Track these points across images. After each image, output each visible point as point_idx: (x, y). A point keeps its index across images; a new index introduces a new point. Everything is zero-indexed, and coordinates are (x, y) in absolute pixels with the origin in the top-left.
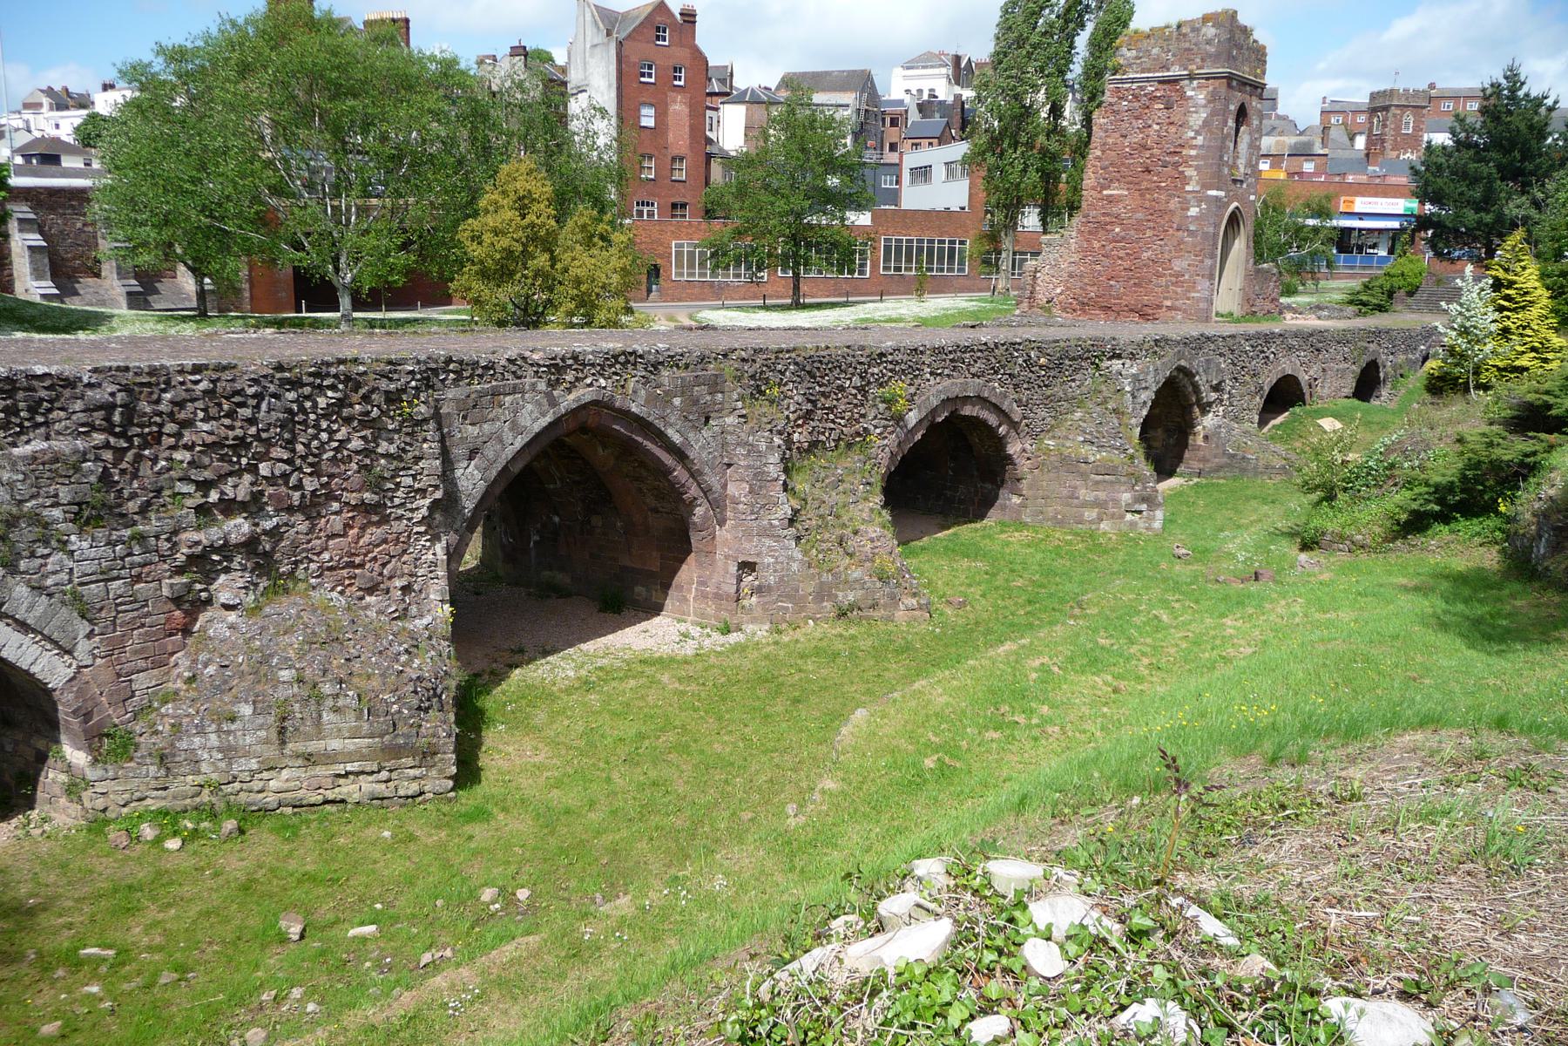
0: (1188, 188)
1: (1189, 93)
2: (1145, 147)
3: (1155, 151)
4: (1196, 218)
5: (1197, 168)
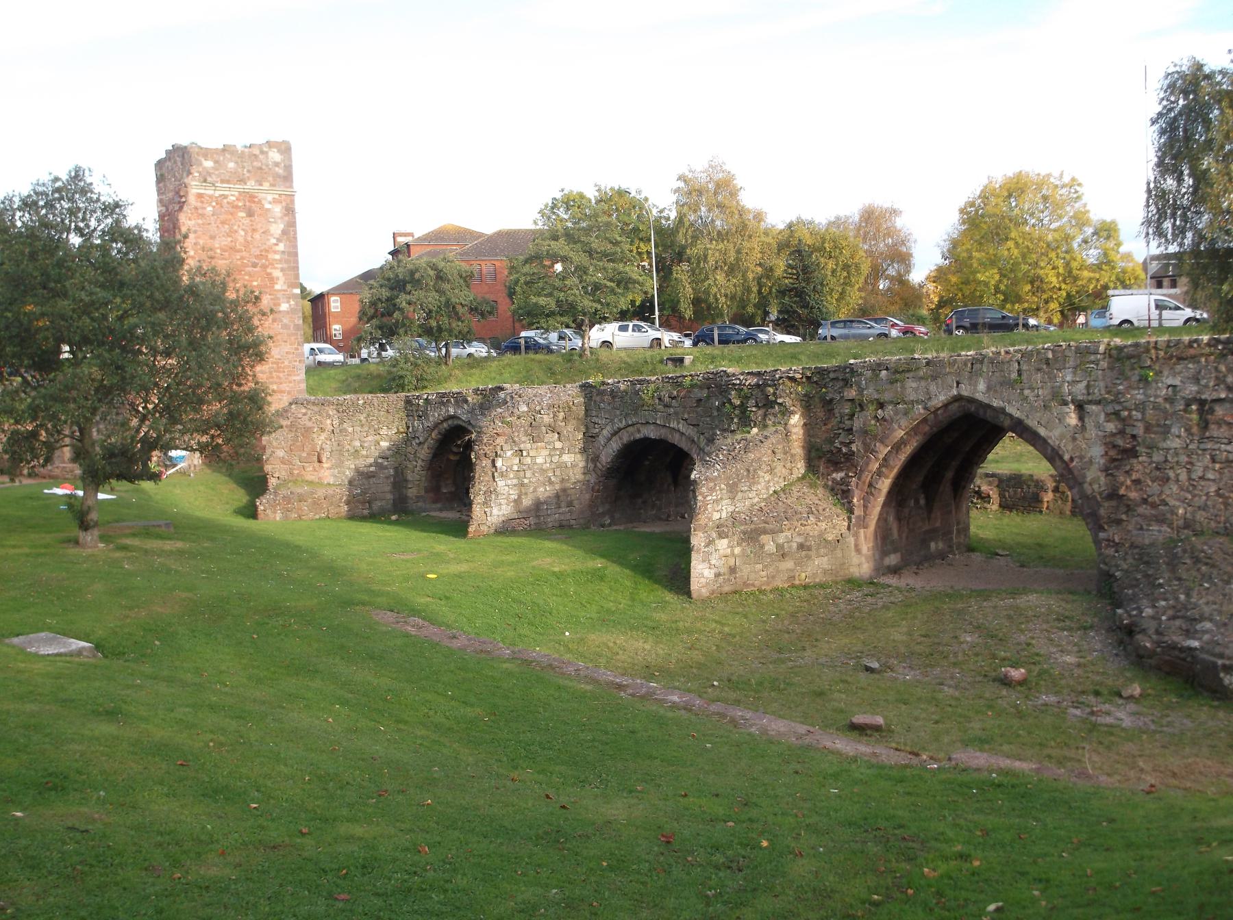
0: (277, 287)
1: (267, 206)
2: (233, 249)
3: (244, 254)
4: (288, 312)
5: (282, 270)
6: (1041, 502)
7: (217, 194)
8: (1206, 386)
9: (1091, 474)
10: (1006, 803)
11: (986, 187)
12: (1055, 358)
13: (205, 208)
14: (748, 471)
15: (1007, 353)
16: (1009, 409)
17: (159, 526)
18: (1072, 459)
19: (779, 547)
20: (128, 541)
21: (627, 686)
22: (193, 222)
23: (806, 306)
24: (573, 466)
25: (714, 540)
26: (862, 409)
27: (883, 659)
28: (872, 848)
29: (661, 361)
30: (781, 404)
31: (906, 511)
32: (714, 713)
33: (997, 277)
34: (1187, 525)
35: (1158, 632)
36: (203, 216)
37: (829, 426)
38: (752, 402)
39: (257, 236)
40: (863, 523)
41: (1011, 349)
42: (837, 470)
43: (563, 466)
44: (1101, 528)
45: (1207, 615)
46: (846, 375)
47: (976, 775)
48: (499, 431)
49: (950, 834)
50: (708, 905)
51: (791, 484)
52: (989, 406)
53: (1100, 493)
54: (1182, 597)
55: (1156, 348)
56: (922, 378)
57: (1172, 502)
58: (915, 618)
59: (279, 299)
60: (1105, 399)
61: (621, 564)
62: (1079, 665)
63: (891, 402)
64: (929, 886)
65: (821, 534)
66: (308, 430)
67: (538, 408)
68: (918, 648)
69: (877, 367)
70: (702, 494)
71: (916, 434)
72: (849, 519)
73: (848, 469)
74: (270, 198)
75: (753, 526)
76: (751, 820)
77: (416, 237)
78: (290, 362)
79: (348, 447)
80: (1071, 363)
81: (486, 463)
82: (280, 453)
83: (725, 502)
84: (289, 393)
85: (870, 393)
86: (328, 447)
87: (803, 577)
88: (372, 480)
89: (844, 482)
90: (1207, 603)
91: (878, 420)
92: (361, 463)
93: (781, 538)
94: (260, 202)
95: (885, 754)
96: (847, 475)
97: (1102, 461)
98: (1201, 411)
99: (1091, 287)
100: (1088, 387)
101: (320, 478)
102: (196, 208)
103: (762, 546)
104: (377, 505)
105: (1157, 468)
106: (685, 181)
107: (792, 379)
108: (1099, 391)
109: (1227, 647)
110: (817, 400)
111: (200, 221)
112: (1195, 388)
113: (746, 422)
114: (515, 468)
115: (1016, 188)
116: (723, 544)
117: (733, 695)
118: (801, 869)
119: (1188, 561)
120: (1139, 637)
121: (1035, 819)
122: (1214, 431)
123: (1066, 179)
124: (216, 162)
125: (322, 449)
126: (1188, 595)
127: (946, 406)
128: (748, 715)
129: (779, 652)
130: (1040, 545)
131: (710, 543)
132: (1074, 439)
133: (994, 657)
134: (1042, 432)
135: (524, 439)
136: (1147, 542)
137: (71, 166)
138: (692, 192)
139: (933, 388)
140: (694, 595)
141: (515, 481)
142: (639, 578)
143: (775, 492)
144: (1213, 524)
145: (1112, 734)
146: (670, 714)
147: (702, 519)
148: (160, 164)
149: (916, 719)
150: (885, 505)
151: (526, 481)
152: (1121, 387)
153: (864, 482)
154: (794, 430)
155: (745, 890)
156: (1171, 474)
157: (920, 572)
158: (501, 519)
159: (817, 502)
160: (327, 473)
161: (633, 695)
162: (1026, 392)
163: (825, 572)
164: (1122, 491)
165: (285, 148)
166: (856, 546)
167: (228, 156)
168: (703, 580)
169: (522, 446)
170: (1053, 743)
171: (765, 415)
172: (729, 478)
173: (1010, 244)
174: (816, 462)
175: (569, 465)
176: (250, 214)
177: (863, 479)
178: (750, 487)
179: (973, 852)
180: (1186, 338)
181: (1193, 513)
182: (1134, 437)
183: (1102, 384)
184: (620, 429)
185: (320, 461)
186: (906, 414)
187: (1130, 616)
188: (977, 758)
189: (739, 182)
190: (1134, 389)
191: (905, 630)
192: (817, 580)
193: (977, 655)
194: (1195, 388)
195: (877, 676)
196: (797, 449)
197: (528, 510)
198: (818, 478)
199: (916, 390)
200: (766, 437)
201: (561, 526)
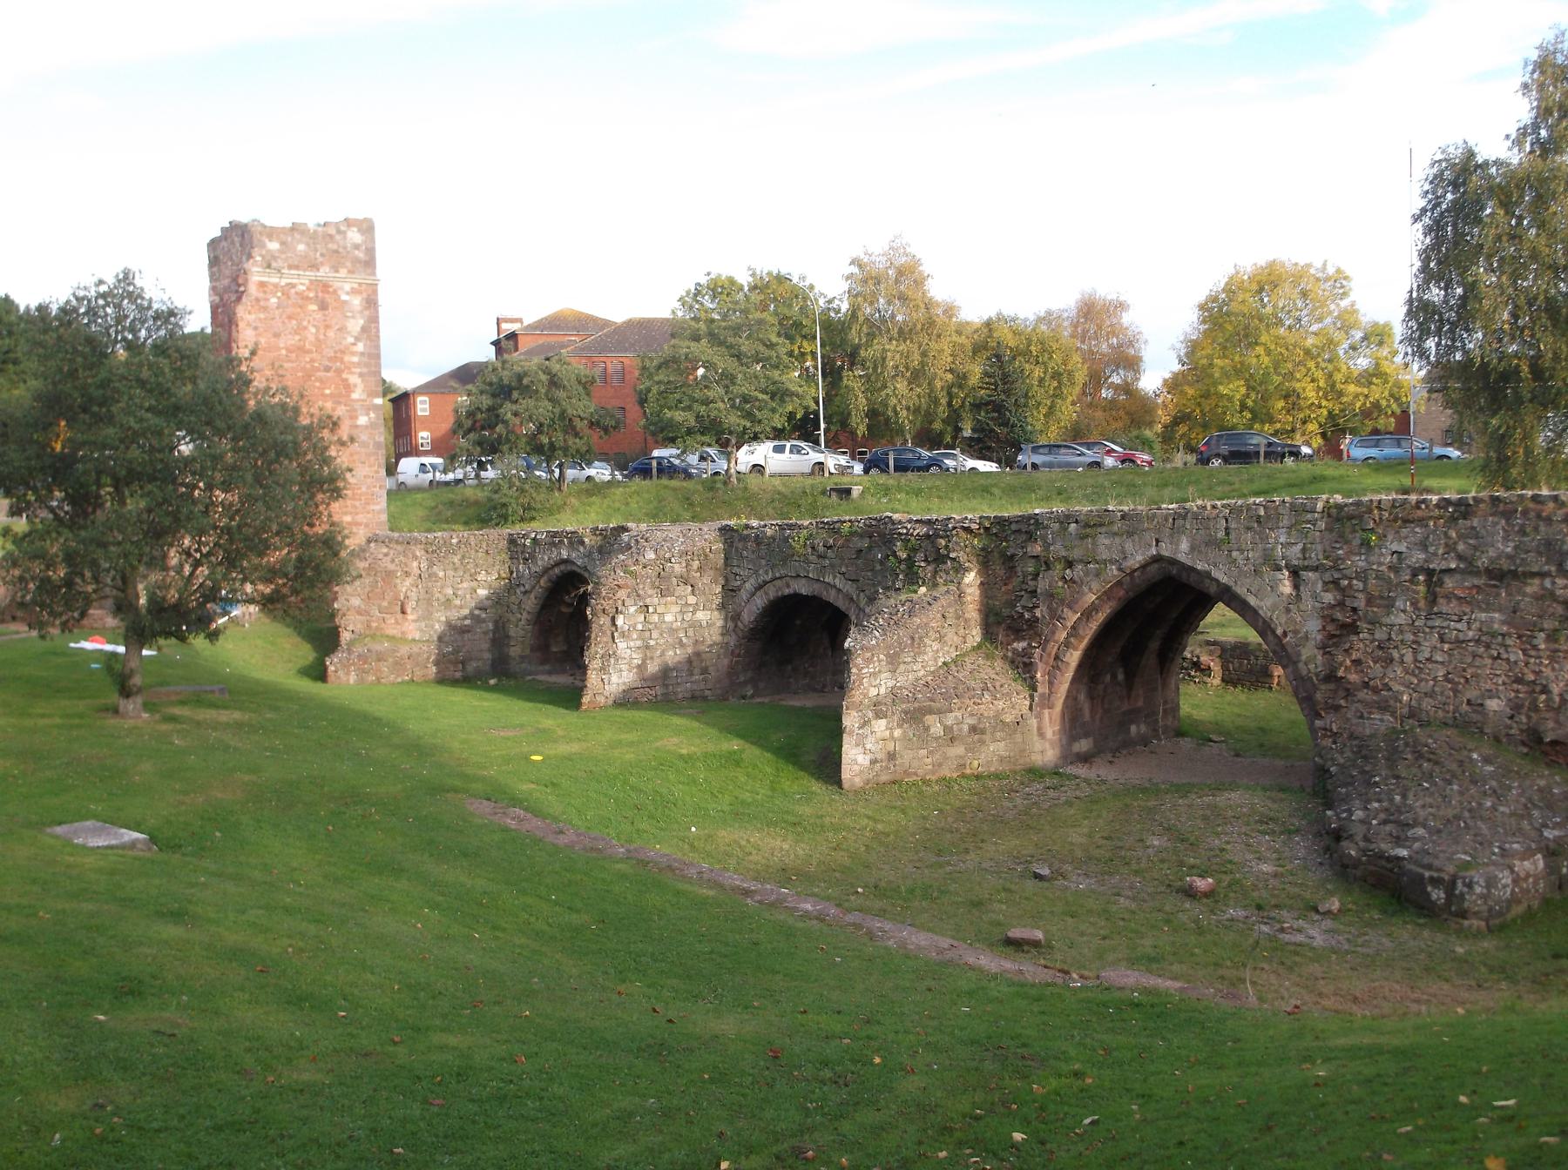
0: (355, 396)
1: (344, 297)
2: (301, 350)
4: (366, 427)
5: (361, 375)
6: (1271, 676)
7: (284, 282)
8: (1435, 554)
9: (1308, 652)
10: (1140, 1023)
11: (1231, 278)
12: (1268, 516)
13: (267, 300)
14: (913, 638)
15: (1214, 507)
16: (1215, 574)
17: (212, 692)
18: (1285, 634)
19: (947, 729)
20: (177, 711)
21: (755, 892)
22: (253, 316)
23: (1006, 424)
24: (709, 625)
25: (869, 721)
26: (1048, 568)
27: (1056, 865)
28: (988, 1066)
29: (823, 493)
30: (954, 559)
31: (1101, 687)
32: (850, 924)
33: (1243, 390)
34: (1412, 714)
35: (1366, 839)
36: (265, 309)
37: (1010, 587)
38: (920, 556)
39: (331, 334)
40: (1047, 702)
41: (1219, 503)
42: (1018, 639)
43: (696, 625)
44: (1318, 716)
45: (1421, 819)
46: (1029, 527)
47: (1118, 994)
48: (621, 582)
49: (1072, 1052)
50: (807, 1116)
51: (963, 655)
52: (1192, 569)
53: (1317, 675)
54: (1398, 798)
55: (1379, 508)
56: (1115, 534)
57: (1396, 687)
58: (1099, 816)
59: (355, 410)
60: (1322, 564)
61: (762, 746)
62: (1276, 875)
63: (1081, 561)
64: (1034, 1101)
65: (998, 714)
66: (390, 574)
67: (667, 556)
68: (1096, 853)
69: (1065, 520)
70: (856, 666)
71: (1109, 599)
72: (1032, 697)
73: (1031, 639)
74: (347, 287)
75: (916, 705)
76: (869, 1038)
77: (526, 323)
78: (368, 488)
79: (437, 595)
80: (1285, 522)
81: (604, 620)
82: (356, 602)
83: (883, 676)
84: (367, 525)
85: (1058, 549)
86: (413, 595)
87: (976, 764)
88: (466, 636)
89: (1026, 653)
90: (1423, 806)
91: (1066, 582)
92: (454, 615)
93: (950, 719)
94: (335, 292)
95: (1030, 970)
96: (1030, 645)
97: (1319, 637)
98: (1429, 583)
99: (1358, 405)
100: (1304, 550)
101: (403, 633)
102: (257, 300)
103: (927, 729)
104: (472, 666)
105: (1380, 647)
106: (860, 266)
107: (968, 530)
108: (1316, 556)
109: (1436, 857)
111: (262, 316)
112: (1422, 556)
113: (913, 579)
114: (640, 627)
115: (1268, 280)
116: (880, 725)
117: (878, 904)
118: (910, 1086)
119: (1409, 756)
120: (1344, 844)
121: (1163, 1039)
122: (1443, 606)
123: (1331, 270)
124: (283, 243)
125: (407, 597)
126: (1404, 796)
127: (1144, 567)
128: (888, 926)
129: (939, 855)
130: (1262, 729)
131: (865, 724)
132: (1288, 611)
133: (1181, 864)
134: (1252, 601)
135: (650, 592)
136: (1368, 732)
137: (119, 269)
138: (867, 280)
139: (1129, 546)
140: (846, 785)
141: (639, 643)
142: (782, 764)
143: (945, 663)
144: (1440, 713)
145: (1297, 953)
146: (800, 925)
147: (856, 695)
148: (213, 244)
149: (1082, 934)
150: (1074, 680)
151: (652, 643)
152: (1340, 552)
153: (1049, 655)
154: (969, 591)
155: (848, 1104)
156: (1396, 655)
157: (1116, 760)
158: (621, 689)
159: (993, 676)
160: (412, 626)
161: (760, 902)
162: (1235, 554)
163: (1001, 759)
164: (1341, 673)
165: (367, 227)
166: (1039, 729)
167: (297, 236)
168: (856, 768)
169: (648, 601)
170: (1229, 963)
171: (936, 572)
172: (889, 647)
173: (1260, 350)
175: (704, 624)
176: (323, 306)
178: (914, 657)
179: (1089, 1071)
180: (1413, 498)
181: (1419, 701)
182: (1354, 610)
183: (1319, 547)
184: (766, 583)
185: (403, 612)
186: (1098, 575)
187: (1339, 819)
188: (1128, 976)
189: (926, 268)
190: (1356, 554)
191: (1086, 830)
192: (992, 769)
193: (1162, 861)
194: (1422, 556)
195: (1046, 884)
196: (972, 613)
197: (654, 678)
198: (996, 648)
199: (1109, 548)
200: (935, 599)
201: (693, 698)
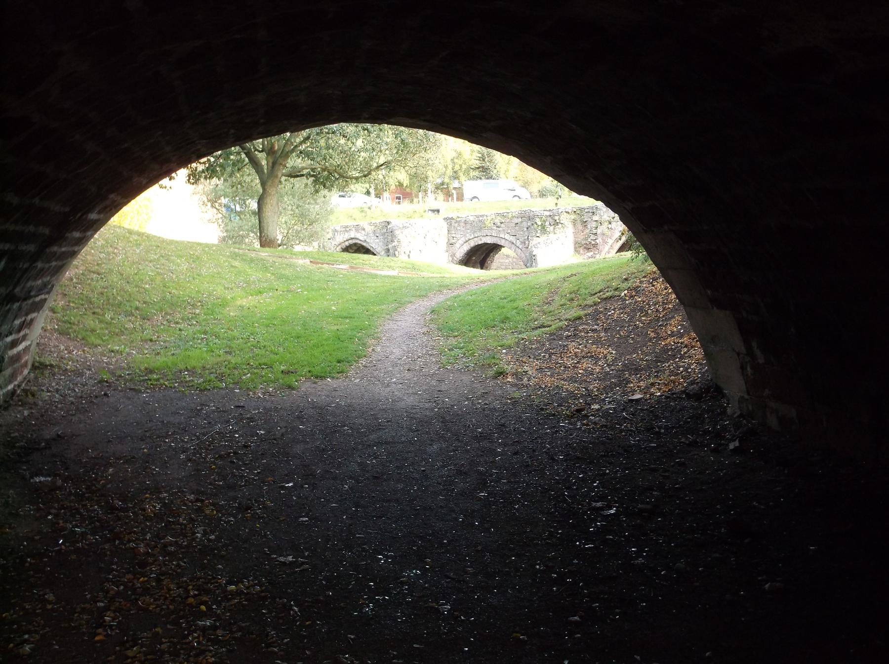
38: (547, 223)
110: (579, 221)
174: (578, 249)
177: (602, 255)
184: (469, 239)
